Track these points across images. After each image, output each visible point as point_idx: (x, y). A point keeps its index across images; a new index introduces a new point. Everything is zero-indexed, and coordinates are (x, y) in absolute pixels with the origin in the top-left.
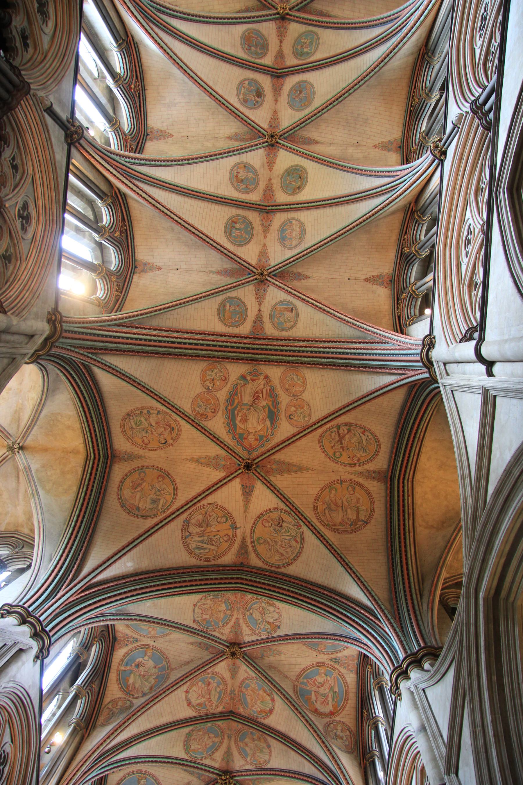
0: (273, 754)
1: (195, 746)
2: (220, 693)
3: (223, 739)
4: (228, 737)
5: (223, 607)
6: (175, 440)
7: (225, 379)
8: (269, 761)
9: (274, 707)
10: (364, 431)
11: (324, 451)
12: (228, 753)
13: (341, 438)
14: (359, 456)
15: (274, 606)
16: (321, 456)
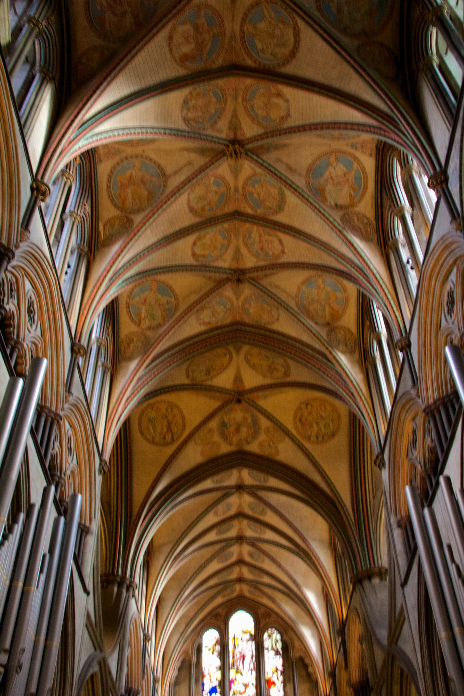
0: (186, 205)
1: (275, 192)
2: (250, 237)
3: (244, 188)
4: (238, 190)
5: (252, 311)
6: (299, 408)
7: (261, 445)
8: (189, 194)
9: (192, 250)
10: (153, 438)
11: (181, 411)
12: (236, 172)
13: (169, 428)
14: (153, 412)
15: (204, 324)
16: (181, 405)
